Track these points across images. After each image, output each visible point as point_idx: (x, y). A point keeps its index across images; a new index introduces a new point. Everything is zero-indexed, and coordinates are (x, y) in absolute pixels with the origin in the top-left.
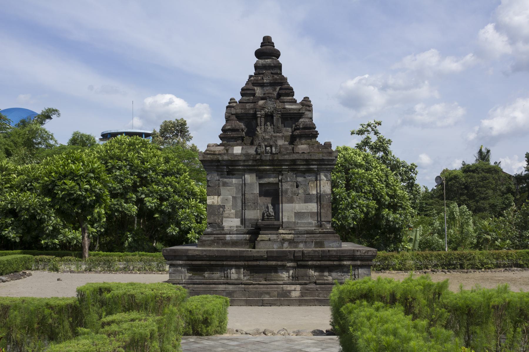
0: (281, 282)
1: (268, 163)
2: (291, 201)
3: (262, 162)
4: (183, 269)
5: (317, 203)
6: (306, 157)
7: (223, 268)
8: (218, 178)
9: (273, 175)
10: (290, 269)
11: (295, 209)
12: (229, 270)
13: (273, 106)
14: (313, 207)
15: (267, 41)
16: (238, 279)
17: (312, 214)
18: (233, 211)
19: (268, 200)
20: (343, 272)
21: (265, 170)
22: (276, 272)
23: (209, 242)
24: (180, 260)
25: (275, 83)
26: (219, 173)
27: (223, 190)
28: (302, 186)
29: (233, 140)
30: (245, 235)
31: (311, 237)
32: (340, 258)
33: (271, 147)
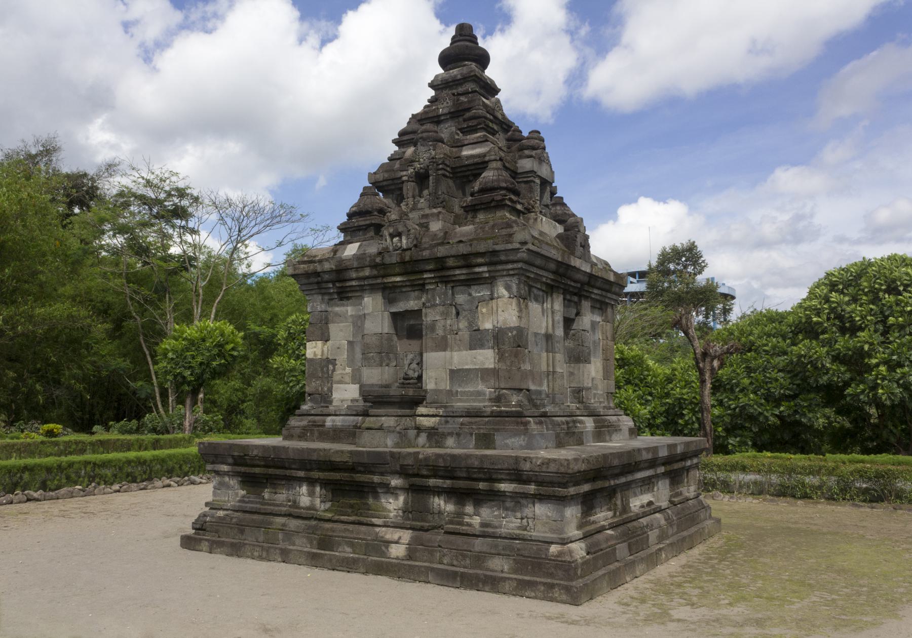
1: (397, 270)
2: (443, 345)
4: (231, 482)
6: (463, 249)
8: (321, 307)
9: (413, 294)
10: (399, 492)
12: (298, 488)
14: (486, 358)
16: (312, 508)
17: (485, 374)
18: (348, 370)
20: (506, 509)
21: (394, 287)
23: (298, 431)
25: (458, 111)
26: (326, 297)
27: (334, 329)
28: (464, 313)
30: (356, 418)
31: (471, 423)
33: (399, 235)
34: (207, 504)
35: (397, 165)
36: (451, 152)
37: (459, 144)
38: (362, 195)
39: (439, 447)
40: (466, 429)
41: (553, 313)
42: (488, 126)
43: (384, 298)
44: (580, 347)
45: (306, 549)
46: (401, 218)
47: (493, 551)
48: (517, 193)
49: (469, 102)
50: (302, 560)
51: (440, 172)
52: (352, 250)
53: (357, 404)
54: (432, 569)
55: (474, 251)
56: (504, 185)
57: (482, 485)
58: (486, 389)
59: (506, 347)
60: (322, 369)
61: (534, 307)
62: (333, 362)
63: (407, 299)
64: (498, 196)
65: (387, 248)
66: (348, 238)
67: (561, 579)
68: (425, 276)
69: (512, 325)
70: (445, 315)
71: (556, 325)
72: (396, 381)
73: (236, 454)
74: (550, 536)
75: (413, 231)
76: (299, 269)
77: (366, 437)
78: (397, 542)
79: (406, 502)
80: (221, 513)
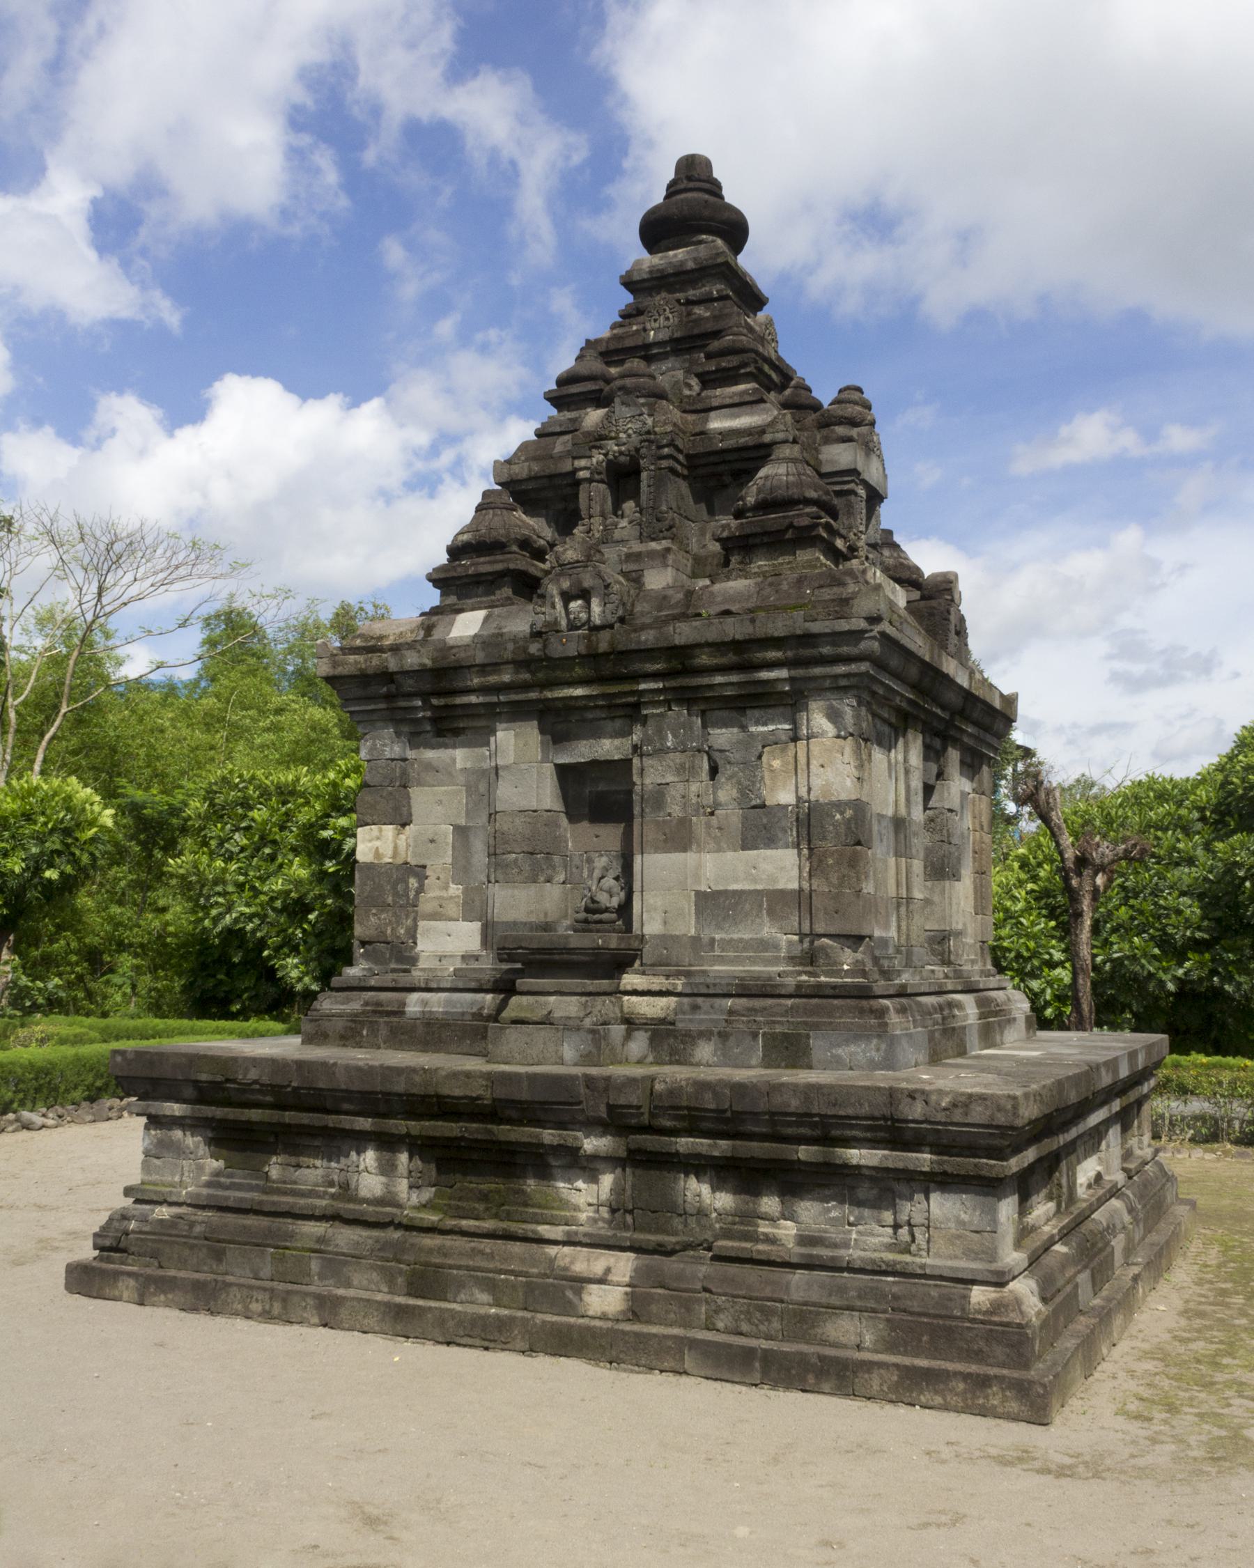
1: (578, 671)
2: (679, 838)
5: (797, 846)
6: (735, 630)
9: (610, 726)
10: (600, 1165)
11: (697, 878)
12: (353, 1154)
13: (639, 425)
14: (781, 867)
17: (776, 902)
18: (455, 890)
20: (859, 1204)
21: (570, 706)
22: (545, 1173)
23: (340, 1024)
26: (406, 729)
27: (421, 798)
28: (730, 770)
29: (481, 589)
30: (479, 996)
31: (752, 1010)
32: (829, 1131)
33: (585, 595)
34: (128, 1191)
35: (561, 445)
36: (686, 422)
37: (699, 406)
38: (479, 509)
39: (678, 1063)
40: (741, 1024)
41: (907, 772)
42: (760, 370)
43: (542, 731)
44: (946, 846)
45: (379, 1297)
46: (589, 558)
47: (834, 1301)
48: (834, 514)
49: (715, 318)
50: (371, 1322)
51: (664, 463)
52: (467, 625)
53: (476, 965)
54: (694, 1344)
56: (812, 494)
57: (804, 1153)
58: (782, 936)
59: (828, 845)
60: (394, 888)
61: (878, 755)
62: (420, 871)
63: (597, 734)
64: (802, 517)
65: (556, 622)
66: (452, 599)
67: (1003, 1366)
68: (643, 686)
70: (688, 773)
71: (913, 798)
72: (565, 917)
73: (204, 1077)
74: (965, 1265)
75: (616, 587)
76: (343, 664)
77: (514, 1038)
78: (602, 1281)
79: (617, 1190)
80: (163, 1212)
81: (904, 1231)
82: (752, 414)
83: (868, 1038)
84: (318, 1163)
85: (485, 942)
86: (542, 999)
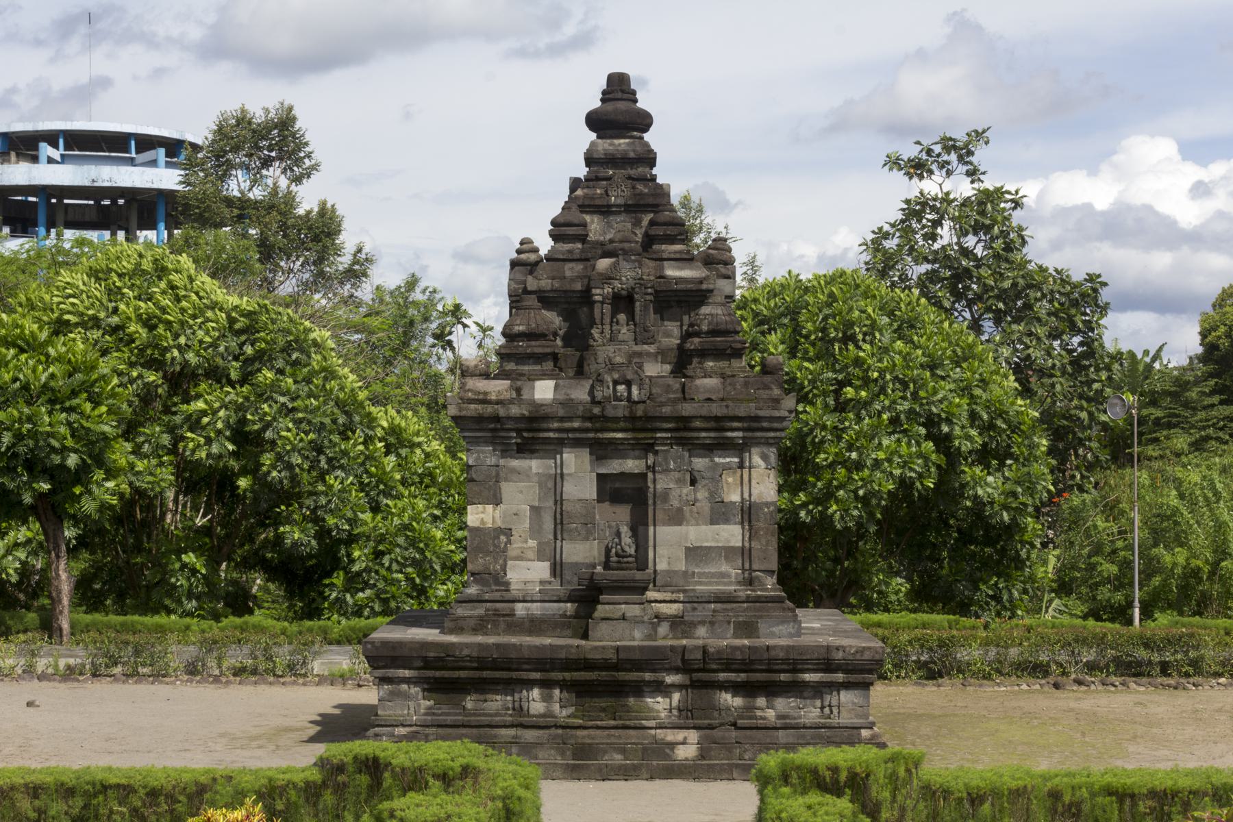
0: (652, 723)
1: (622, 424)
2: (677, 518)
3: (603, 422)
5: (742, 523)
6: (716, 410)
7: (510, 686)
8: (491, 460)
10: (672, 689)
13: (634, 274)
15: (619, 87)
16: (548, 714)
18: (532, 543)
19: (622, 514)
21: (612, 442)
23: (472, 622)
24: (405, 668)
26: (499, 448)
27: (507, 489)
28: (704, 482)
30: (562, 605)
33: (629, 384)
43: (591, 454)
54: (737, 766)
55: (731, 413)
57: (783, 677)
58: (733, 570)
68: (659, 435)
69: (769, 500)
74: (857, 721)
76: (466, 409)
78: (684, 743)
81: (827, 710)
82: (691, 269)
83: (789, 622)
84: (498, 697)
85: (554, 573)
86: (618, 606)
